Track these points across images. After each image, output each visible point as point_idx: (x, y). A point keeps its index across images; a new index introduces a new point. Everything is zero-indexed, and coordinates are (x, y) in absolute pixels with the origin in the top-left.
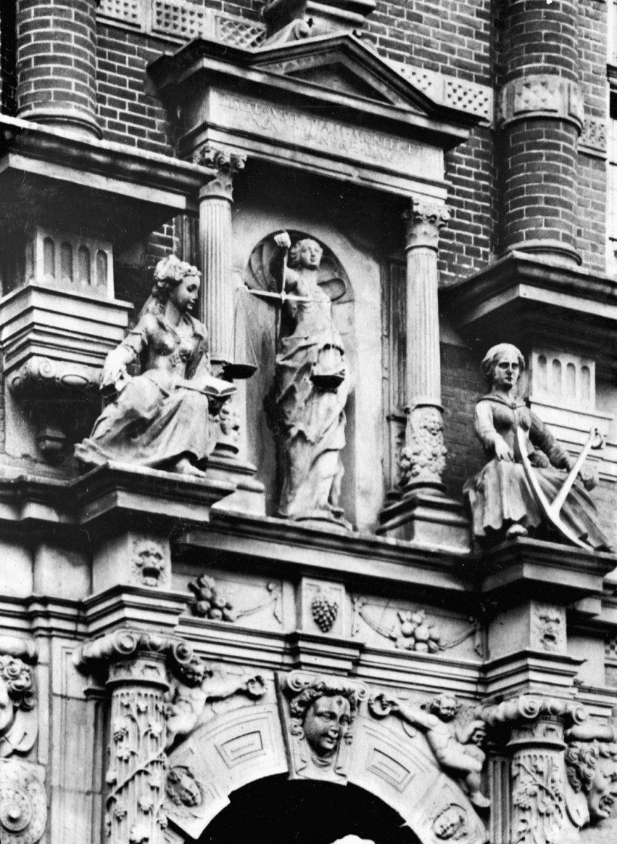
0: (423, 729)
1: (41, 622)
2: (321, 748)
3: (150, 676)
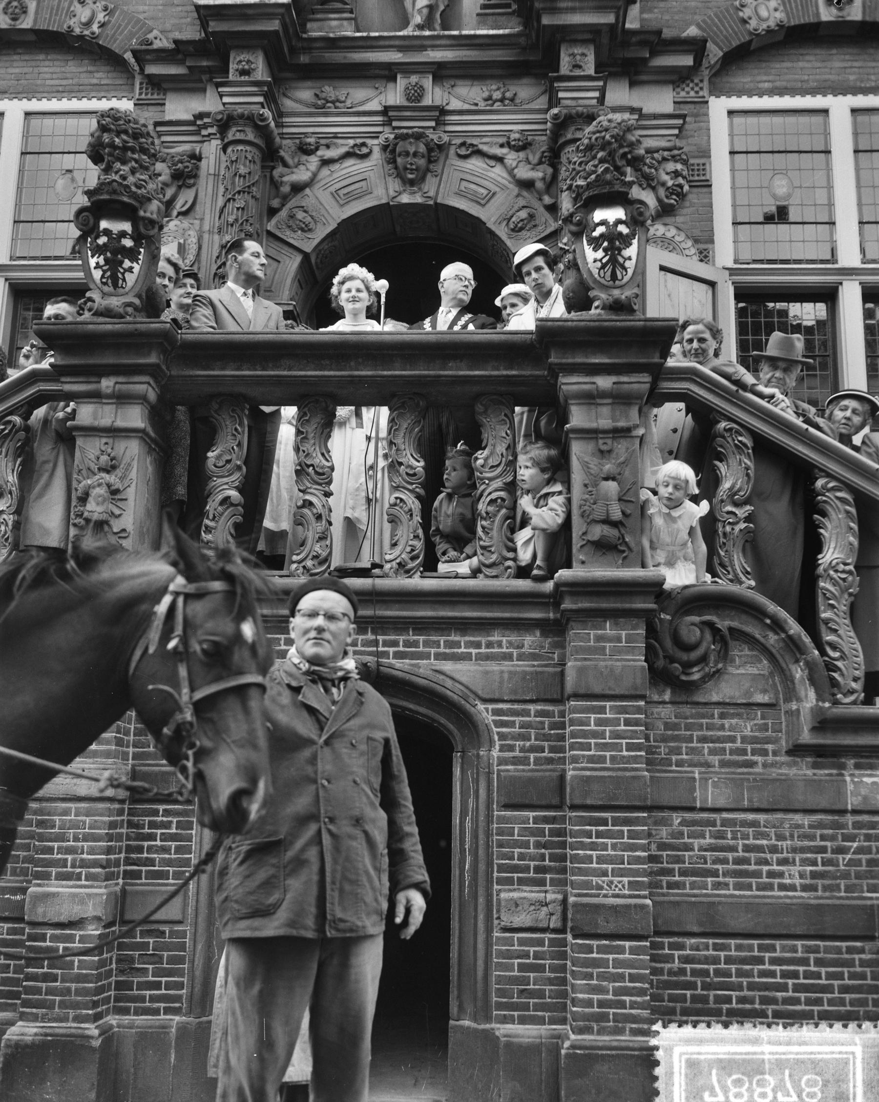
0: (500, 160)
1: (204, 132)
2: (413, 180)
3: (239, 136)
